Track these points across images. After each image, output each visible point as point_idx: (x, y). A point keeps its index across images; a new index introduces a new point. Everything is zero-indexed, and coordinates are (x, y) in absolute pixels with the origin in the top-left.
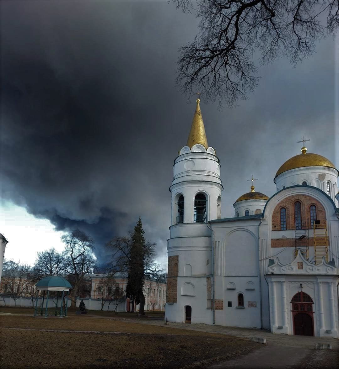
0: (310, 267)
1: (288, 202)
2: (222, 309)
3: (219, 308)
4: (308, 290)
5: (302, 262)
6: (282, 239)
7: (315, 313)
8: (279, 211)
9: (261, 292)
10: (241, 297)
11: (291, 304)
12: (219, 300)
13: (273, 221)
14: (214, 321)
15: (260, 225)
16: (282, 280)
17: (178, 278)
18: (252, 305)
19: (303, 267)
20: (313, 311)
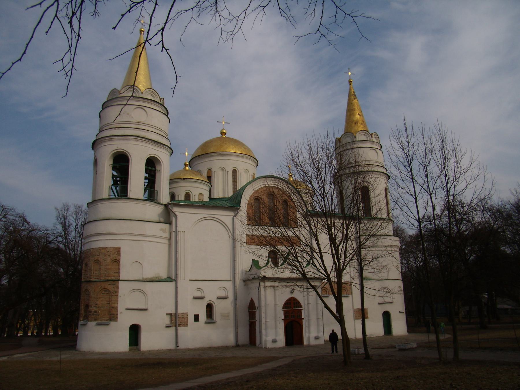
1: (262, 193)
2: (186, 325)
3: (183, 324)
4: (298, 296)
7: (304, 319)
8: (252, 201)
11: (283, 312)
12: (183, 313)
14: (177, 342)
15: (235, 216)
16: (276, 284)
17: (121, 284)
18: (225, 316)
20: (303, 318)
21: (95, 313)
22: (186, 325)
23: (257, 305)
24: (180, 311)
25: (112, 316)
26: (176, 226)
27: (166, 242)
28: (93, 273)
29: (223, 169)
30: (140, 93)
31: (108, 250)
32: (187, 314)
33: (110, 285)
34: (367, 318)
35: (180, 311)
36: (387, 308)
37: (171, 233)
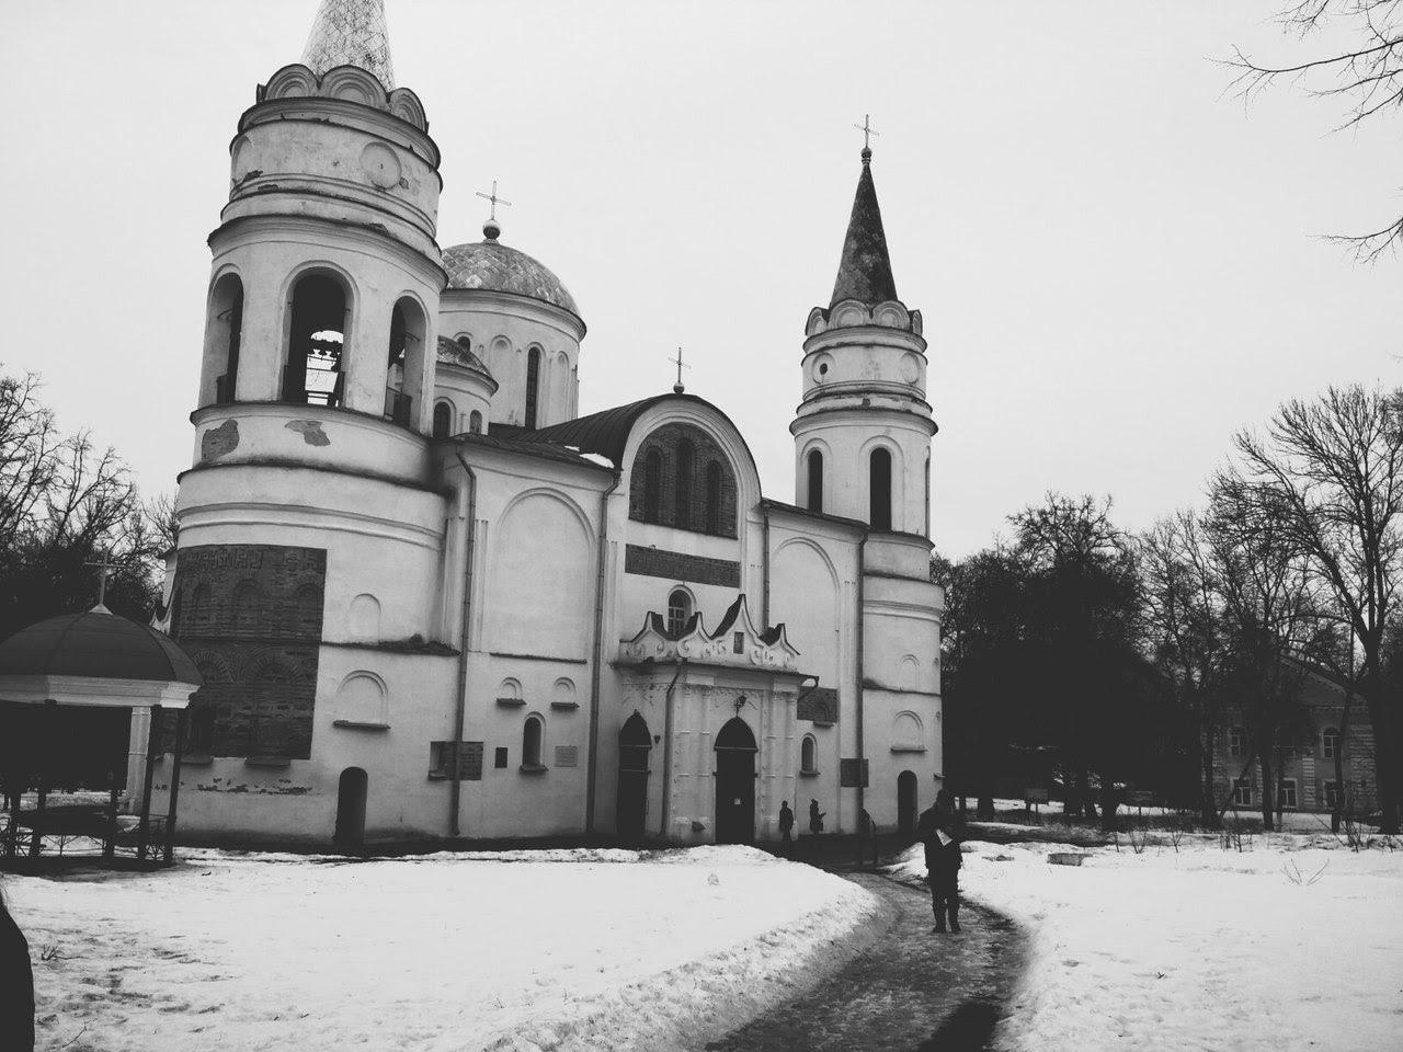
0: (758, 649)
2: (476, 774)
5: (742, 634)
6: (649, 550)
9: (595, 713)
10: (532, 728)
13: (632, 488)
16: (709, 682)
17: (325, 657)
18: (566, 756)
19: (741, 646)
21: (241, 733)
22: (476, 774)
23: (655, 727)
24: (468, 736)
25: (299, 743)
26: (471, 506)
27: (434, 544)
28: (235, 617)
29: (501, 342)
30: (383, 99)
31: (287, 555)
32: (480, 745)
33: (292, 657)
34: (867, 785)
35: (468, 736)
36: (910, 764)
37: (447, 521)
